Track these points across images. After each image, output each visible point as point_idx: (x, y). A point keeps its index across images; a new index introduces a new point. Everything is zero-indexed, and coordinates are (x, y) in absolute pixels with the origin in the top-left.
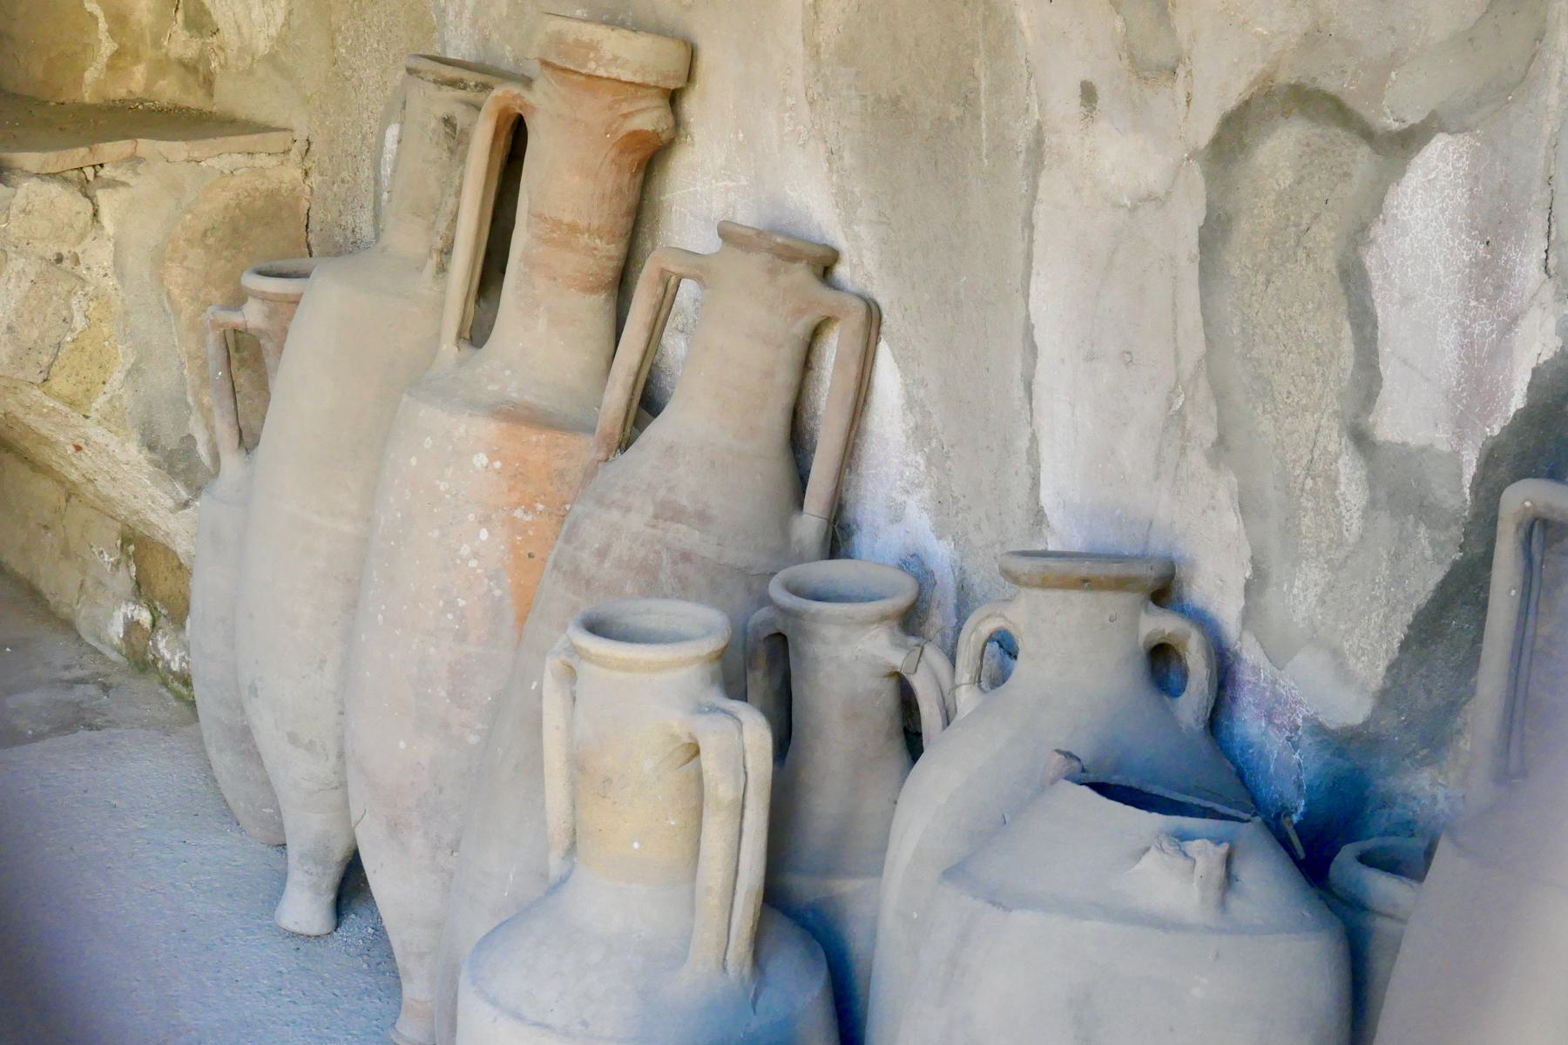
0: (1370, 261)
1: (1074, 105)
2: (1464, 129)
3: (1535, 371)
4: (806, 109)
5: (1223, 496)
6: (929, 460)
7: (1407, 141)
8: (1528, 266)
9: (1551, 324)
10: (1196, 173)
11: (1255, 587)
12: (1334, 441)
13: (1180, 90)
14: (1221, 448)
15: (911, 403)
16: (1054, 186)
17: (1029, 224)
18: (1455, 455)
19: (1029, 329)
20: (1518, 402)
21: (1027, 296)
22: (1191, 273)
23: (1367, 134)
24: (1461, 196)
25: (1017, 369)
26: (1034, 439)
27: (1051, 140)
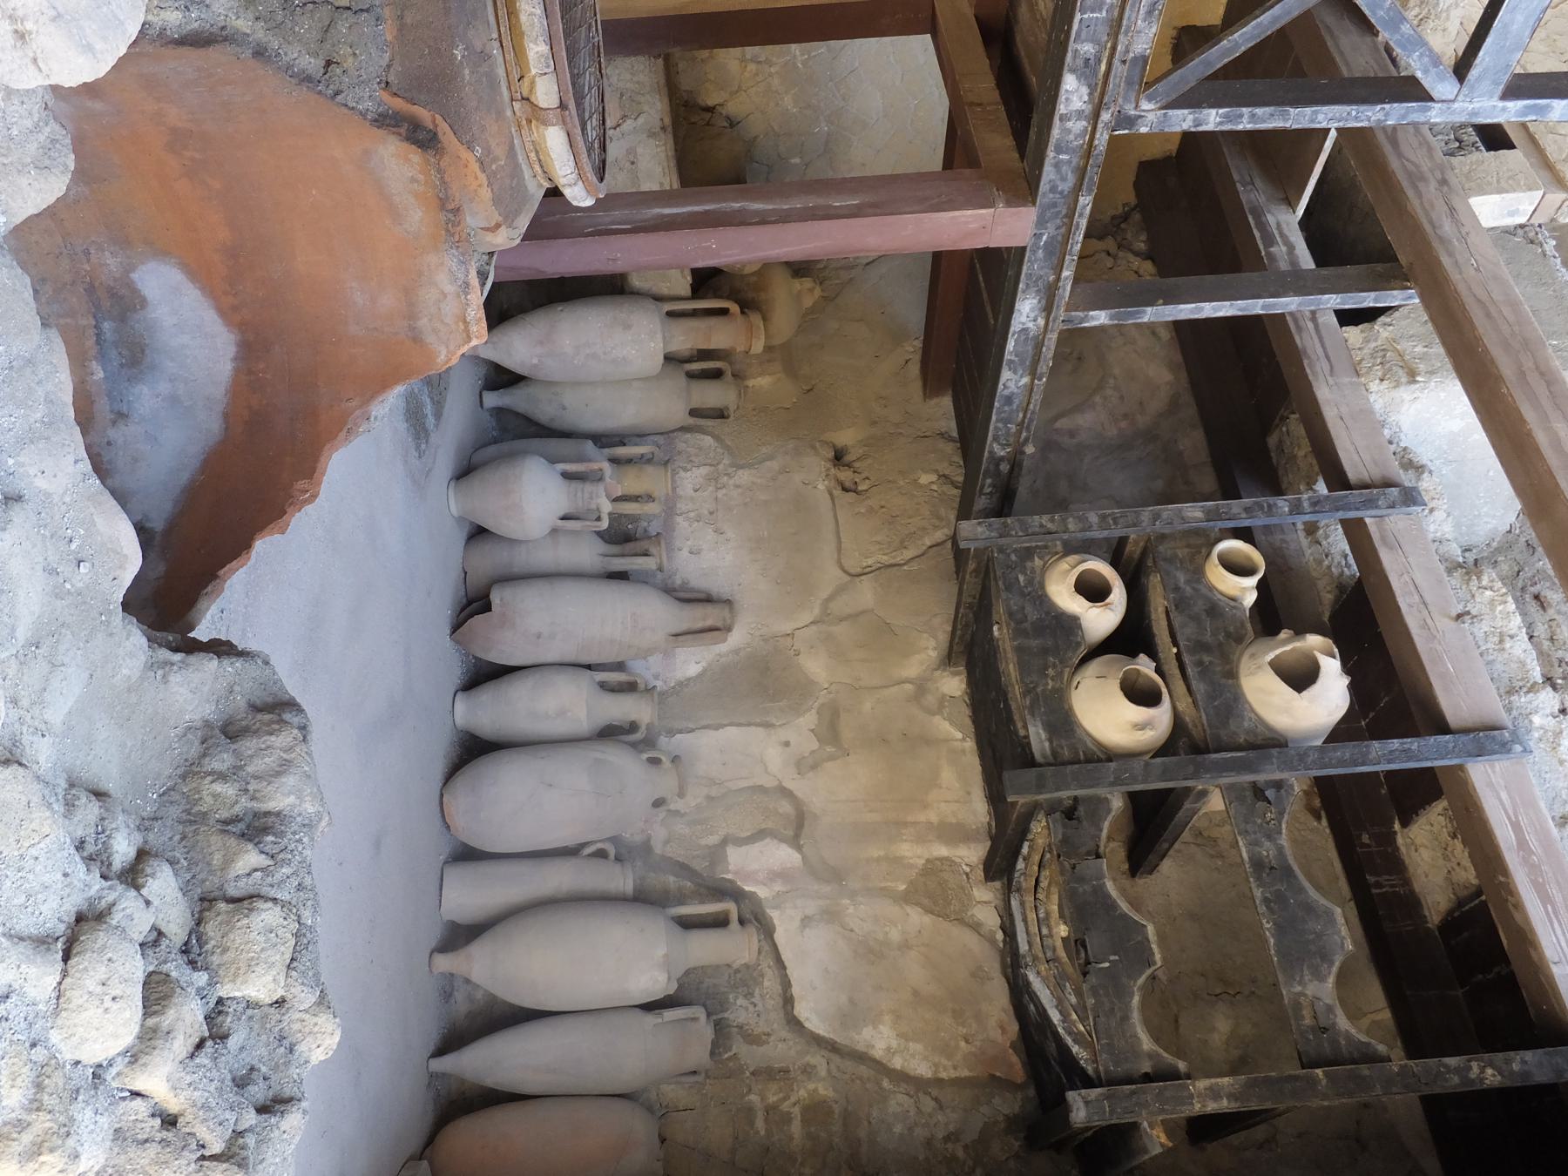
0: (768, 840)
1: (784, 739)
2: (804, 864)
3: (755, 893)
4: (758, 633)
5: (699, 800)
6: (673, 688)
7: (799, 848)
8: (778, 887)
9: (767, 895)
10: (776, 783)
11: (677, 813)
12: (722, 833)
13: (796, 776)
14: (710, 798)
15: (689, 679)
16: (760, 731)
17: (749, 725)
18: (728, 872)
19: (722, 726)
20: (747, 888)
21: (731, 724)
22: (751, 784)
23: (797, 836)
24: (789, 865)
25: (711, 722)
26: (692, 731)
27: (773, 732)
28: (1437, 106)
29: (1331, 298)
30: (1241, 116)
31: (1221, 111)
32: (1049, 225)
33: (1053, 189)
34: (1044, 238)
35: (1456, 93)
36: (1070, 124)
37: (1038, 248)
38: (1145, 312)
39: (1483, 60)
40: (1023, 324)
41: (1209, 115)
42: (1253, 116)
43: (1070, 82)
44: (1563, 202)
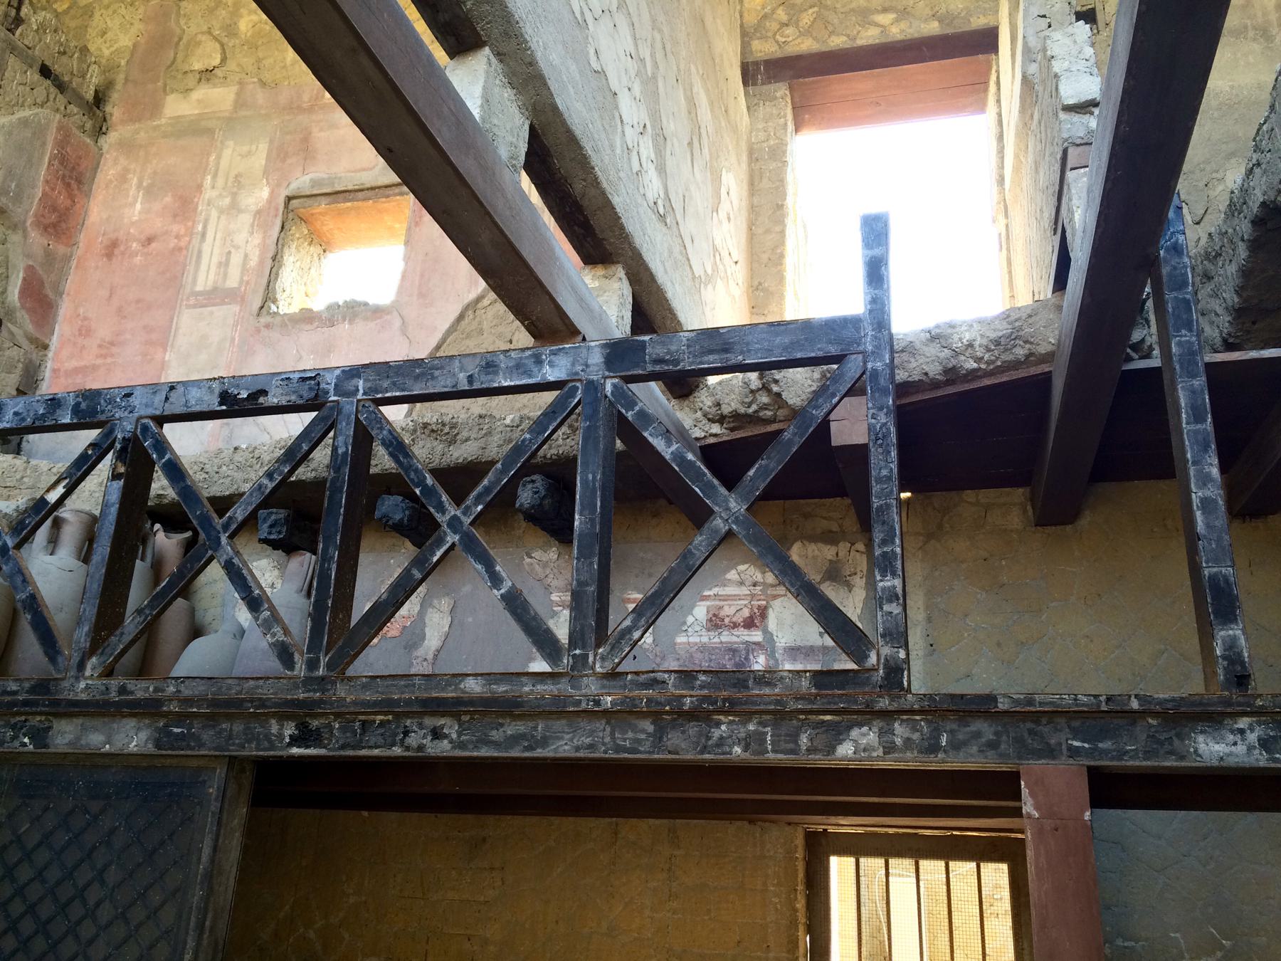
28: (869, 365)
29: (1179, 344)
30: (884, 554)
31: (878, 578)
32: (1053, 742)
33: (993, 745)
34: (1076, 744)
35: (855, 356)
36: (898, 741)
37: (1096, 749)
38: (1213, 578)
39: (819, 349)
40: (1250, 748)
41: (884, 589)
42: (884, 542)
43: (845, 750)
44: (1078, 145)
